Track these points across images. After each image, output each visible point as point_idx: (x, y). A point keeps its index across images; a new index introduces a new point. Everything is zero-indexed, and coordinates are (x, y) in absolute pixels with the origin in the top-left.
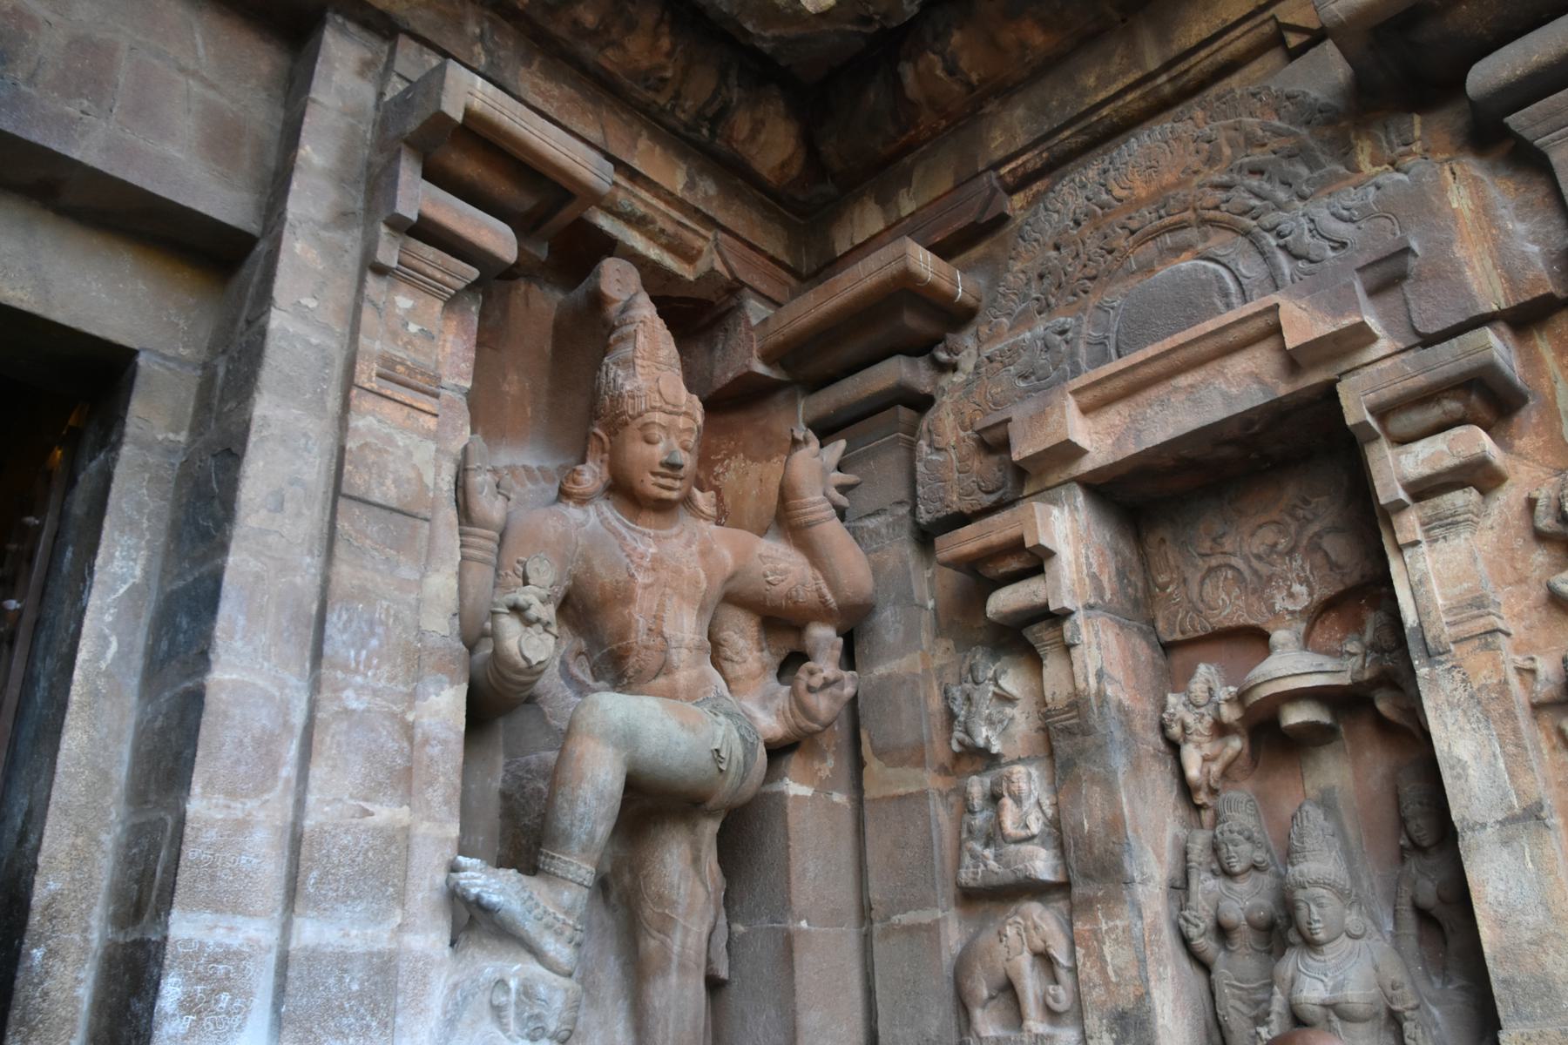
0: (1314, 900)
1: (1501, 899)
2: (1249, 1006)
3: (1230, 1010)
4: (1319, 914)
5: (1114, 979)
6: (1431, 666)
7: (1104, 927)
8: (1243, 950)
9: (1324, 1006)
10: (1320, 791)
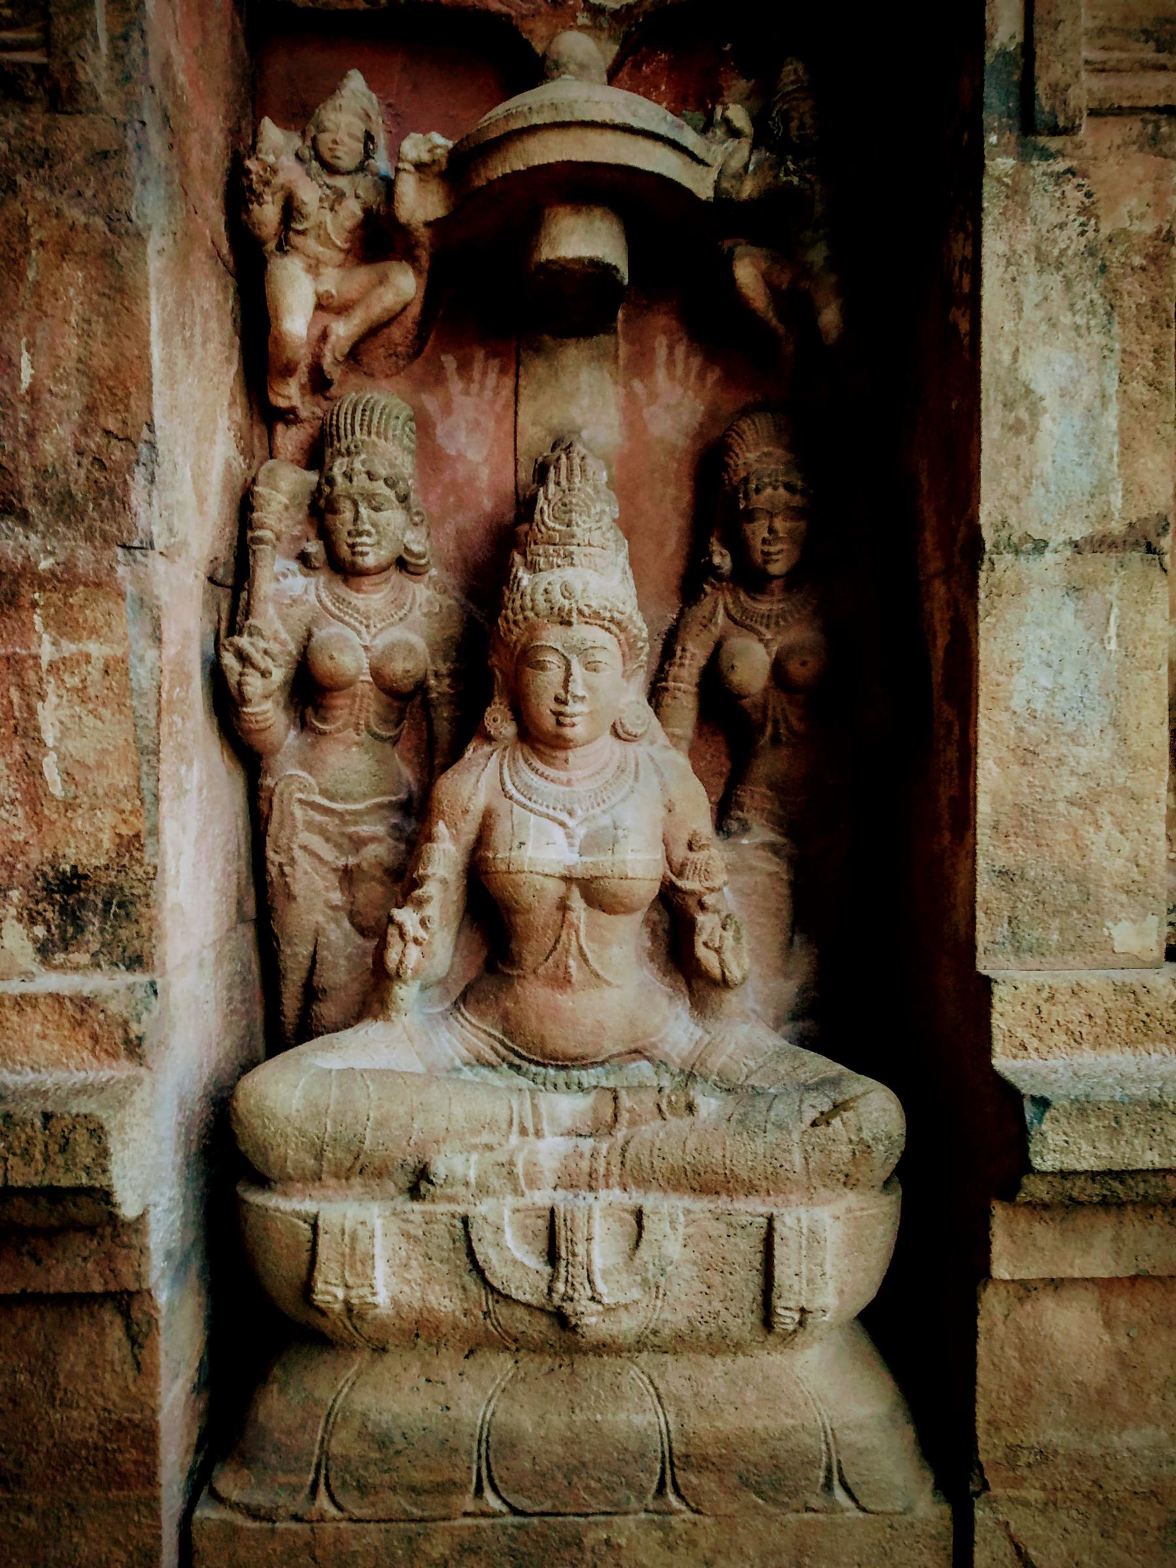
0: (582, 652)
1: (1039, 705)
2: (338, 846)
3: (298, 853)
4: (590, 688)
5: (57, 790)
6: (1025, 153)
7: (46, 652)
8: (350, 734)
9: (567, 879)
10: (550, 431)
